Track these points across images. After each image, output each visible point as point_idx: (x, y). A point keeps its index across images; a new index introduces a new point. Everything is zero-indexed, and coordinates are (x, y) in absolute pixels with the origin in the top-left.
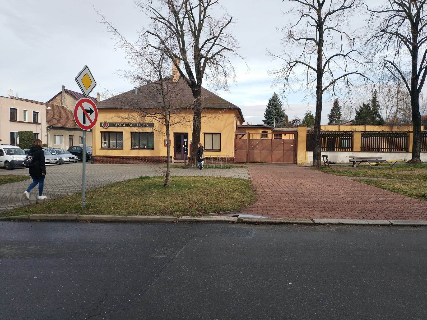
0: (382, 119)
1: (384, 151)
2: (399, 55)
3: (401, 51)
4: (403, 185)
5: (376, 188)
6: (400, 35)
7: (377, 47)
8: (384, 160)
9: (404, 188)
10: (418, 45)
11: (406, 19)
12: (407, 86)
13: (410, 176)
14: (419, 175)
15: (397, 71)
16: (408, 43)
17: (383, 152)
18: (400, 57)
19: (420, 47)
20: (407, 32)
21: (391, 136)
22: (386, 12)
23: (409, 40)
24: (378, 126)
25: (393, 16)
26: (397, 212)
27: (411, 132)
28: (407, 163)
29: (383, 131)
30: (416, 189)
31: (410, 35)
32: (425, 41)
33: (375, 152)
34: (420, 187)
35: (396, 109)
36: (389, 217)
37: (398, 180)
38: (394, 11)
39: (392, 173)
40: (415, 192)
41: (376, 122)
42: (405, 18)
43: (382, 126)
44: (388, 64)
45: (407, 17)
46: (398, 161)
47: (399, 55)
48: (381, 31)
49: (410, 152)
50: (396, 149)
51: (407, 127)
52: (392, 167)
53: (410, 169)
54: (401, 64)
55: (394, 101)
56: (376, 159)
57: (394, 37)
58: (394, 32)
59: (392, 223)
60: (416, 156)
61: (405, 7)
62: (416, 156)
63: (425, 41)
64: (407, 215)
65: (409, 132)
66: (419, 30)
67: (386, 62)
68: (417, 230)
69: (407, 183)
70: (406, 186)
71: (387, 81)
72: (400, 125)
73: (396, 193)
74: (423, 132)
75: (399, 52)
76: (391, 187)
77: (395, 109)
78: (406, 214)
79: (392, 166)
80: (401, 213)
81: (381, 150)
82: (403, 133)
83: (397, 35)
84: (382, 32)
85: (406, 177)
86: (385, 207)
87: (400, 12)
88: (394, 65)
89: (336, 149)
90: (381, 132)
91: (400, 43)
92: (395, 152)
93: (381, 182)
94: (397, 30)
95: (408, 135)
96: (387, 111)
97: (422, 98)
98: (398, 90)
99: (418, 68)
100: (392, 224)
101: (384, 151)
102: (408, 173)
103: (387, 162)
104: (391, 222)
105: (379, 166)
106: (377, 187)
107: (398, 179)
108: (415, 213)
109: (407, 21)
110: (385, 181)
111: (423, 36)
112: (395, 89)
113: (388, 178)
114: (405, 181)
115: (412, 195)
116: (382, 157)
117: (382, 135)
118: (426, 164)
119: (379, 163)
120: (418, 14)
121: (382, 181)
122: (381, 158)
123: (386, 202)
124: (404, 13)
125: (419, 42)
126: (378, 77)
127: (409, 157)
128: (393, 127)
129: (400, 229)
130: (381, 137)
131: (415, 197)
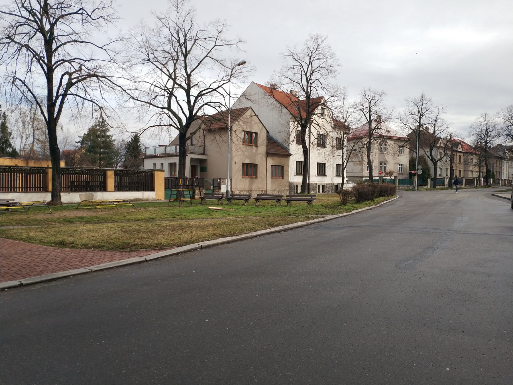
0: (14, 151)
1: (18, 191)
2: (31, 74)
3: (34, 70)
4: (39, 232)
5: (4, 239)
6: (32, 49)
7: (2, 57)
8: (17, 203)
9: (40, 235)
10: (54, 67)
11: (38, 33)
12: (42, 113)
13: (48, 220)
14: (58, 218)
15: (29, 93)
16: (41, 62)
17: (16, 192)
18: (32, 76)
19: (55, 70)
20: (40, 48)
21: (27, 172)
22: (13, 16)
23: (42, 58)
24: (8, 159)
25: (21, 23)
26: (29, 267)
27: (50, 168)
28: (46, 204)
29: (16, 166)
30: (54, 235)
31: (43, 52)
32: (61, 64)
33: (5, 192)
34: (59, 232)
35: (32, 140)
36: (19, 276)
37: (34, 227)
38: (22, 17)
39: (28, 218)
40: (53, 239)
41: (6, 153)
42: (37, 30)
43: (14, 160)
44: (18, 82)
45: (39, 30)
46: (34, 203)
47: (31, 74)
48: (6, 38)
49: (50, 192)
50: (32, 188)
51: (45, 162)
52: (28, 211)
53: (49, 212)
54: (34, 85)
55: (29, 129)
56: (7, 202)
57: (24, 50)
58: (24, 44)
59: (22, 282)
60: (56, 196)
61: (36, 18)
62: (56, 196)
63: (61, 64)
64: (41, 269)
65: (48, 168)
66: (53, 50)
67: (15, 79)
68: (52, 286)
69: (44, 229)
70: (43, 234)
71: (17, 103)
72: (38, 160)
73: (30, 243)
74: (63, 168)
75: (31, 70)
76: (24, 236)
77: (31, 139)
78: (40, 267)
79: (27, 209)
80: (35, 268)
81: (14, 190)
82: (40, 169)
83: (28, 49)
84: (8, 40)
85: (44, 222)
86: (14, 264)
87: (30, 22)
88: (25, 85)
89: (1, 189)
90: (12, 167)
91: (32, 59)
92: (31, 192)
93: (12, 231)
94: (28, 42)
95: (46, 172)
96: (21, 140)
97: (62, 130)
98: (34, 117)
99: (55, 94)
100: (22, 283)
101: (18, 191)
102: (46, 217)
103: (21, 205)
104: (20, 282)
105: (10, 210)
106: (6, 238)
107: (34, 225)
108: (51, 264)
109: (39, 35)
110: (18, 230)
111: (58, 58)
112: (29, 115)
113: (22, 225)
114: (42, 228)
115: (49, 244)
116: (14, 199)
117: (14, 170)
118: (67, 205)
119: (11, 207)
120: (51, 30)
121: (13, 229)
122: (13, 200)
123: (16, 256)
124: (34, 23)
125: (55, 63)
126: (4, 96)
127: (48, 197)
128: (29, 162)
129: (31, 288)
130: (13, 174)
131: (53, 245)
